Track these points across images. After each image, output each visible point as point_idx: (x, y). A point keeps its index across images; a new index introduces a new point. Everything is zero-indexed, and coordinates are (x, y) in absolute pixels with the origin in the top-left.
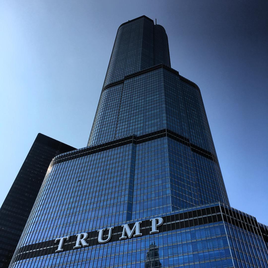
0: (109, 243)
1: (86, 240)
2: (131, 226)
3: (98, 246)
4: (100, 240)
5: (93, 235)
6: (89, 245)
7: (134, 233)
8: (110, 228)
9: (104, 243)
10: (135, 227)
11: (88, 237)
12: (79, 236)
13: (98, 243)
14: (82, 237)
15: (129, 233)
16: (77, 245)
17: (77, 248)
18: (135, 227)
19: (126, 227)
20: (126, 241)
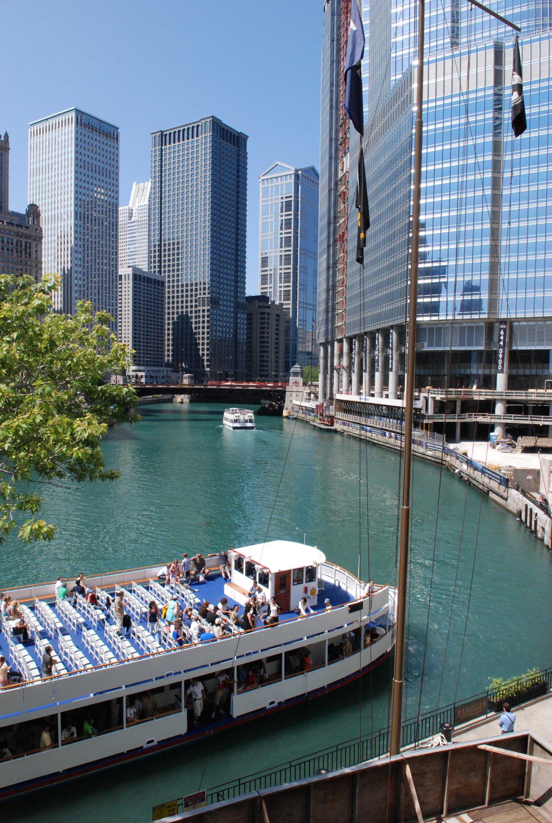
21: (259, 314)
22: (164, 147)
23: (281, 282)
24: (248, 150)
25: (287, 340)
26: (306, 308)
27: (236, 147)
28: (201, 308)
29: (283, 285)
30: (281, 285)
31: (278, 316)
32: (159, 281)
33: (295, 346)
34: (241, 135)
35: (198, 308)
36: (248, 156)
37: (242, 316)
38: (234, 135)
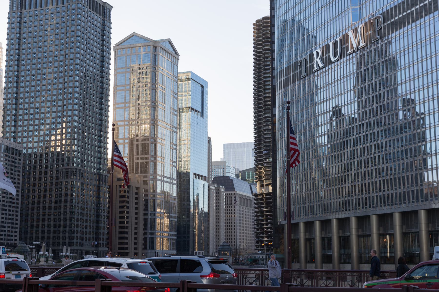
0: (342, 61)
1: (320, 59)
2: (355, 31)
3: (333, 65)
4: (333, 59)
5: (326, 49)
6: (326, 66)
7: (359, 44)
8: (338, 39)
9: (338, 60)
10: (356, 38)
11: (323, 55)
12: (315, 53)
13: (331, 62)
14: (318, 53)
15: (355, 46)
16: (316, 68)
17: (317, 71)
18: (356, 38)
19: (350, 33)
20: (354, 54)
21: (118, 187)
22: (23, 11)
23: (137, 154)
24: (112, 21)
25: (145, 215)
26: (164, 181)
27: (101, 17)
28: (64, 181)
29: (140, 156)
30: (137, 156)
31: (137, 188)
32: (16, 150)
33: (153, 221)
34: (106, 5)
35: (60, 180)
36: (112, 26)
37: (105, 189)
38: (100, 4)
